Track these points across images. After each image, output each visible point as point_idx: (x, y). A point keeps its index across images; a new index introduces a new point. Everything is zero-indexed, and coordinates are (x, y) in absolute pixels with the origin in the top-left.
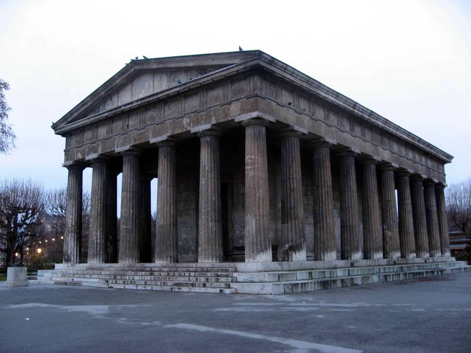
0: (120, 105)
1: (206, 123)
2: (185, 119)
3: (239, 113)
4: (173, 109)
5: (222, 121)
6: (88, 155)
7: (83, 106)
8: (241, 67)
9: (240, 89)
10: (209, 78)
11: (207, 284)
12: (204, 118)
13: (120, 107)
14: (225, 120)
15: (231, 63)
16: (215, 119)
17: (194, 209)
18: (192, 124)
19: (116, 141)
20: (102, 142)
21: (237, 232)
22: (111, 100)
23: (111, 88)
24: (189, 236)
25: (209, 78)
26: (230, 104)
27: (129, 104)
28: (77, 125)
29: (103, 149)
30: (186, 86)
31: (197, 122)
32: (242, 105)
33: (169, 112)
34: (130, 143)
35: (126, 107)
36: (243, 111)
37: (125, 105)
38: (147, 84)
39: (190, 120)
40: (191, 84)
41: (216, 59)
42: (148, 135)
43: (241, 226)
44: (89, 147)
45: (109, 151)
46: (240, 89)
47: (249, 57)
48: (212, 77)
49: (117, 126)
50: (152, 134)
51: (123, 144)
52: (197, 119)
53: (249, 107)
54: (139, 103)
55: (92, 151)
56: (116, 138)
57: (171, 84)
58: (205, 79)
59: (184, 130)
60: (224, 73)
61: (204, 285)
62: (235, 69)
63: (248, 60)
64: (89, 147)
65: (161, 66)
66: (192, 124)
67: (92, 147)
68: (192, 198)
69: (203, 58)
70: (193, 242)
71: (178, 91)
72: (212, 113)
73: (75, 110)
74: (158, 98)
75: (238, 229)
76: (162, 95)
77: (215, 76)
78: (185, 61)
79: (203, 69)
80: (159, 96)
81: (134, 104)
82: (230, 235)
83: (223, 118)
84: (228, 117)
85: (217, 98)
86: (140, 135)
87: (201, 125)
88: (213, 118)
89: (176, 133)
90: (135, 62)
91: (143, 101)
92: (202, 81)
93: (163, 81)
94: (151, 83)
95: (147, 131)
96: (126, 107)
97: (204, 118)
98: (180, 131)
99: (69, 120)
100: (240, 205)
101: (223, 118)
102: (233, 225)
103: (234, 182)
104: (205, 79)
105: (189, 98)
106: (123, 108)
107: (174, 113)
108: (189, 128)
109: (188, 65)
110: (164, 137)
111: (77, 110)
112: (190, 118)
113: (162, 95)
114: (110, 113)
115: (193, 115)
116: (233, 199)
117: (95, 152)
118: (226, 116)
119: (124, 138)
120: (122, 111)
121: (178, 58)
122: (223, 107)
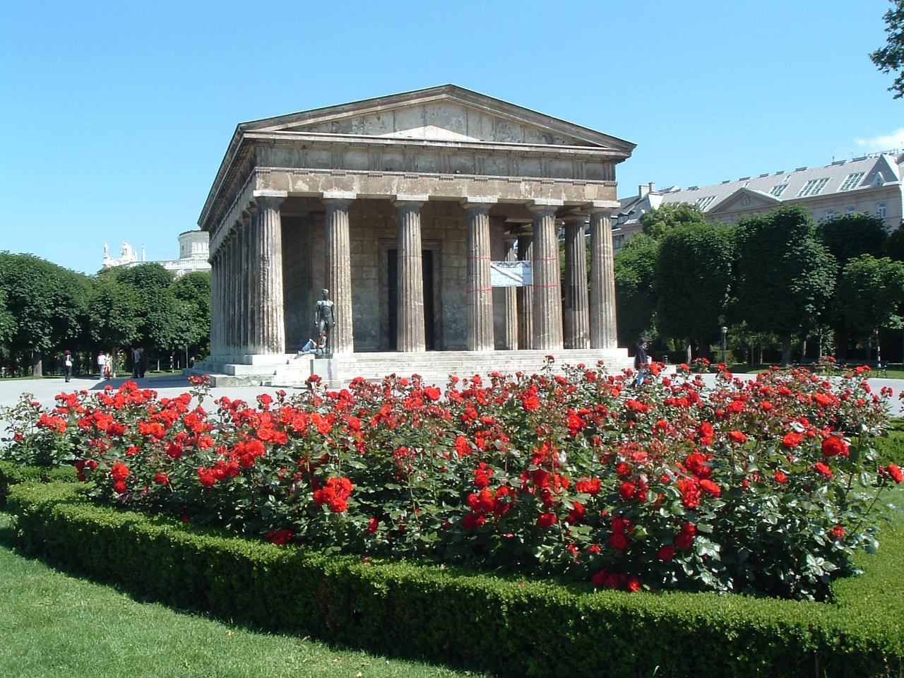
1: (552, 197)
3: (596, 197)
5: (575, 200)
6: (326, 190)
7: (330, 113)
8: (613, 154)
12: (551, 190)
13: (422, 141)
14: (579, 200)
16: (566, 196)
17: (375, 279)
18: (533, 193)
21: (448, 314)
22: (379, 119)
24: (365, 316)
25: (572, 151)
26: (584, 185)
31: (541, 193)
34: (427, 193)
36: (601, 197)
37: (431, 141)
44: (327, 177)
45: (378, 193)
50: (468, 190)
53: (607, 194)
54: (460, 145)
55: (336, 185)
56: (394, 179)
58: (567, 151)
59: (522, 198)
68: (372, 264)
70: (373, 324)
72: (562, 188)
75: (450, 311)
76: (501, 148)
77: (580, 152)
80: (496, 148)
81: (449, 145)
82: (437, 318)
84: (583, 198)
87: (547, 197)
88: (563, 194)
89: (509, 197)
90: (452, 89)
92: (562, 151)
94: (463, 122)
95: (459, 184)
99: (290, 125)
102: (441, 304)
103: (444, 251)
108: (529, 196)
111: (314, 117)
112: (530, 185)
114: (398, 142)
116: (441, 273)
117: (346, 187)
118: (580, 197)
121: (532, 113)
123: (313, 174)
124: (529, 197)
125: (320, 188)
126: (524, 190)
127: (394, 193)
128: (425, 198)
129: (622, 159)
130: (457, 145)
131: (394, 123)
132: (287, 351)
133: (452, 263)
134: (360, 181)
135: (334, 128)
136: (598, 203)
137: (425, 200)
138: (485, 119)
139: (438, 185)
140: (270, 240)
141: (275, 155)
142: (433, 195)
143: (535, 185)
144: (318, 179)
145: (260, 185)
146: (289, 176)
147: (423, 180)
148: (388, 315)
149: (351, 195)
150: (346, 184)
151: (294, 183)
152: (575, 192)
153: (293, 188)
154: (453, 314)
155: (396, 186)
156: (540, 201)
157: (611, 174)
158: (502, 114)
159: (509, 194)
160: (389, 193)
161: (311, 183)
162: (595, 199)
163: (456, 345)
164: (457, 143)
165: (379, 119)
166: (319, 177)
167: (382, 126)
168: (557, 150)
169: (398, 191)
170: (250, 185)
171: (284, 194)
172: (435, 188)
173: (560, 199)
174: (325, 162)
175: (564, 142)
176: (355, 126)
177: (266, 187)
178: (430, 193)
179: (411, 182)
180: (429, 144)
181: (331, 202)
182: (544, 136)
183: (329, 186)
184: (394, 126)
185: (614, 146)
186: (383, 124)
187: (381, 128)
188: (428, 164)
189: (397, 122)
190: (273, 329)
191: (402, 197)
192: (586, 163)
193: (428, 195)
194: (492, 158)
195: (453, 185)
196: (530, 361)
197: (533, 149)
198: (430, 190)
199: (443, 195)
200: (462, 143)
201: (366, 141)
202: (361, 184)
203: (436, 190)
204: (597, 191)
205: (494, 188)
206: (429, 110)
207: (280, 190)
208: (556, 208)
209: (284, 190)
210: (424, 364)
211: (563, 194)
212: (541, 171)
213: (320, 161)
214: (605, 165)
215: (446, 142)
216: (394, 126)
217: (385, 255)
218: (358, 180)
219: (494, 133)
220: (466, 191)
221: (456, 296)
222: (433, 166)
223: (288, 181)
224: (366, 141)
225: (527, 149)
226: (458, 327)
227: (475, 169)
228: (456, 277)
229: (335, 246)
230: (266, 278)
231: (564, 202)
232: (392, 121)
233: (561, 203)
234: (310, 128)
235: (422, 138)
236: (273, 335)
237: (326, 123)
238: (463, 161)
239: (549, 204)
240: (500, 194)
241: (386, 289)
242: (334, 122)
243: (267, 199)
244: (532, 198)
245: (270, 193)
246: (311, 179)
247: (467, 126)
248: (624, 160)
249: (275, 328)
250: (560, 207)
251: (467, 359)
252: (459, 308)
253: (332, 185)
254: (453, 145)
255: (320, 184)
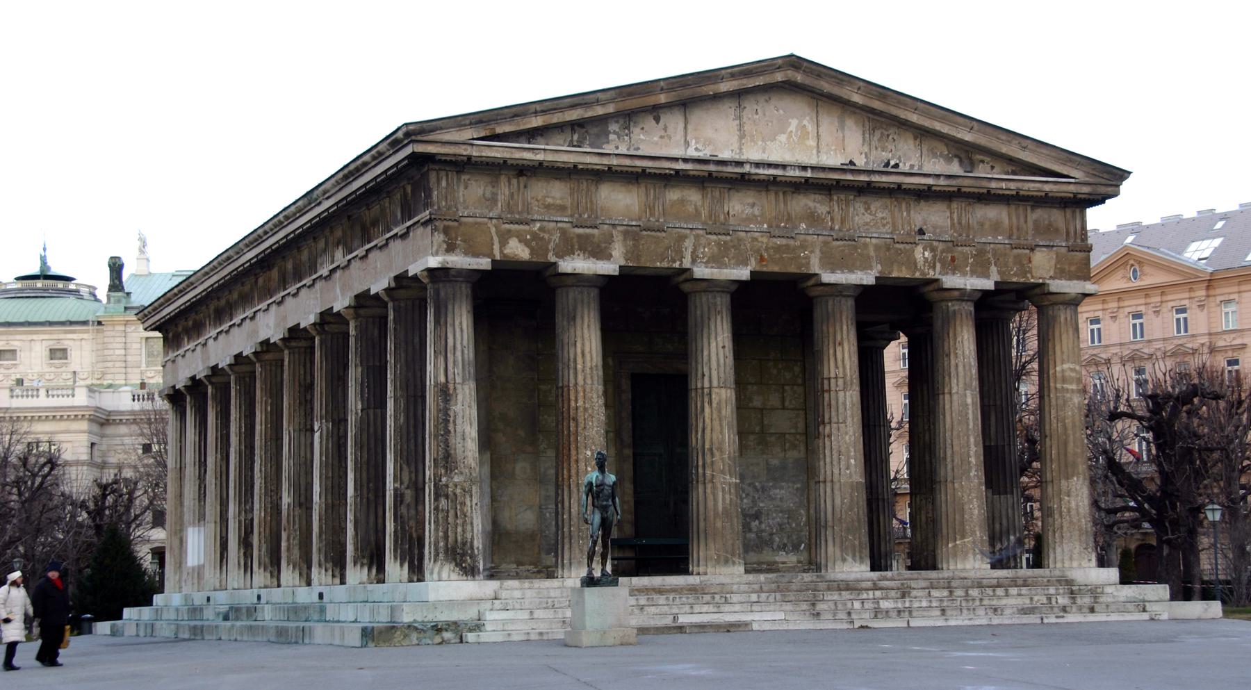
0: (744, 158)
1: (974, 273)
2: (920, 249)
3: (1052, 273)
4: (880, 215)
5: (1015, 280)
6: (561, 256)
7: (573, 107)
8: (1086, 189)
9: (1050, 225)
10: (1013, 186)
11: (1097, 607)
12: (971, 261)
13: (740, 164)
14: (1022, 280)
15: (1065, 173)
18: (938, 266)
19: (688, 244)
20: (626, 234)
22: (657, 120)
23: (689, 94)
25: (1013, 186)
26: (1032, 250)
27: (776, 166)
28: (540, 157)
29: (632, 253)
30: (953, 182)
31: (953, 266)
32: (1058, 260)
33: (868, 218)
35: (761, 171)
36: (1061, 273)
37: (757, 165)
38: (794, 123)
39: (934, 257)
40: (967, 182)
41: (1031, 150)
42: (807, 257)
43: (755, 487)
44: (563, 232)
45: (658, 264)
46: (1050, 225)
47: (1105, 176)
48: (1020, 185)
49: (682, 202)
50: (820, 259)
51: (716, 260)
52: (953, 259)
53: (1073, 268)
54: (809, 174)
56: (686, 237)
57: (873, 152)
58: (1004, 185)
59: (917, 275)
60: (1047, 188)
61: (1092, 610)
62: (1072, 188)
63: (1103, 181)
64: (563, 232)
65: (877, 105)
66: (938, 266)
67: (579, 236)
69: (1004, 137)
71: (930, 187)
73: (538, 108)
74: (869, 183)
75: (747, 495)
78: (934, 118)
79: (967, 152)
83: (1015, 275)
85: (996, 227)
86: (778, 249)
87: (964, 274)
88: (993, 269)
89: (894, 275)
90: (794, 62)
91: (821, 175)
92: (993, 185)
93: (847, 133)
94: (810, 127)
95: (803, 247)
96: (761, 171)
97: (971, 261)
98: (905, 274)
99: (500, 130)
100: (752, 437)
101: (1015, 275)
104: (1004, 185)
105: (922, 203)
106: (747, 168)
107: (884, 225)
108: (932, 273)
109: (959, 136)
110: (867, 278)
112: (933, 250)
113: (884, 179)
115: (941, 246)
117: (599, 252)
118: (1024, 274)
119: (718, 244)
120: (743, 175)
122: (1015, 251)
123: (538, 225)
124: (931, 274)
125: (550, 254)
126: (921, 262)
127: (687, 264)
128: (743, 274)
129: (1099, 200)
130: (803, 174)
131: (685, 128)
132: (491, 577)
133: (751, 400)
134: (625, 240)
135: (576, 137)
136: (1058, 285)
137: (744, 278)
138: (850, 123)
139: (767, 249)
140: (459, 354)
141: (466, 188)
142: (758, 269)
143: (942, 252)
144: (546, 236)
145: (439, 246)
146: (493, 230)
147: (740, 240)
148: (632, 504)
149: (608, 268)
150: (599, 246)
151: (503, 243)
152: (1015, 264)
153: (501, 252)
154: (754, 501)
155: (690, 250)
156: (952, 281)
157: (1079, 227)
158: (882, 110)
159: (895, 267)
160: (677, 265)
161: (534, 244)
162: (1051, 278)
163: (759, 563)
164: (804, 168)
165: (657, 120)
166: (549, 232)
167: (663, 133)
168: (985, 184)
169: (694, 261)
170: (396, 245)
171: (484, 263)
172: (761, 256)
173: (987, 277)
174: (558, 202)
175: (992, 167)
176: (615, 132)
177: (450, 249)
178: (753, 265)
179: (718, 244)
180: (754, 171)
181: (570, 281)
182: (956, 156)
183: (567, 249)
184: (686, 136)
185: (1087, 174)
186: (665, 129)
187: (662, 137)
188: (748, 211)
189: (689, 127)
190: (464, 531)
191: (701, 272)
192: (1033, 208)
193: (749, 268)
194: (863, 199)
195: (795, 248)
196: (946, 593)
197: (942, 182)
198: (753, 260)
199: (776, 269)
200: (813, 168)
201: (639, 163)
202: (625, 246)
203: (762, 259)
204: (1053, 262)
205: (869, 257)
206: (750, 105)
207: (476, 255)
208: (980, 295)
209: (485, 255)
210: (754, 597)
211: (993, 269)
212: (953, 225)
213: (549, 200)
214: (1069, 212)
215: (784, 167)
216: (686, 136)
217: (626, 385)
218: (621, 238)
219: (866, 150)
220: (817, 261)
221: (758, 464)
222: (757, 213)
223: (492, 239)
224: (639, 163)
225: (930, 181)
226: (763, 526)
227: (832, 219)
228: (758, 429)
229: (579, 367)
230: (451, 428)
231: (996, 283)
232: (681, 125)
233: (988, 284)
234: (532, 134)
235: (737, 157)
236: (464, 544)
237: (560, 127)
238: (811, 204)
239: (969, 287)
240: (879, 267)
241: (628, 452)
242: (576, 125)
243: (452, 272)
244: (937, 276)
245: (459, 261)
246: (535, 236)
247: (818, 136)
248: (1102, 202)
249: (469, 528)
250: (985, 293)
251: (829, 589)
252: (763, 489)
253: (572, 246)
254: (797, 173)
255: (551, 246)
